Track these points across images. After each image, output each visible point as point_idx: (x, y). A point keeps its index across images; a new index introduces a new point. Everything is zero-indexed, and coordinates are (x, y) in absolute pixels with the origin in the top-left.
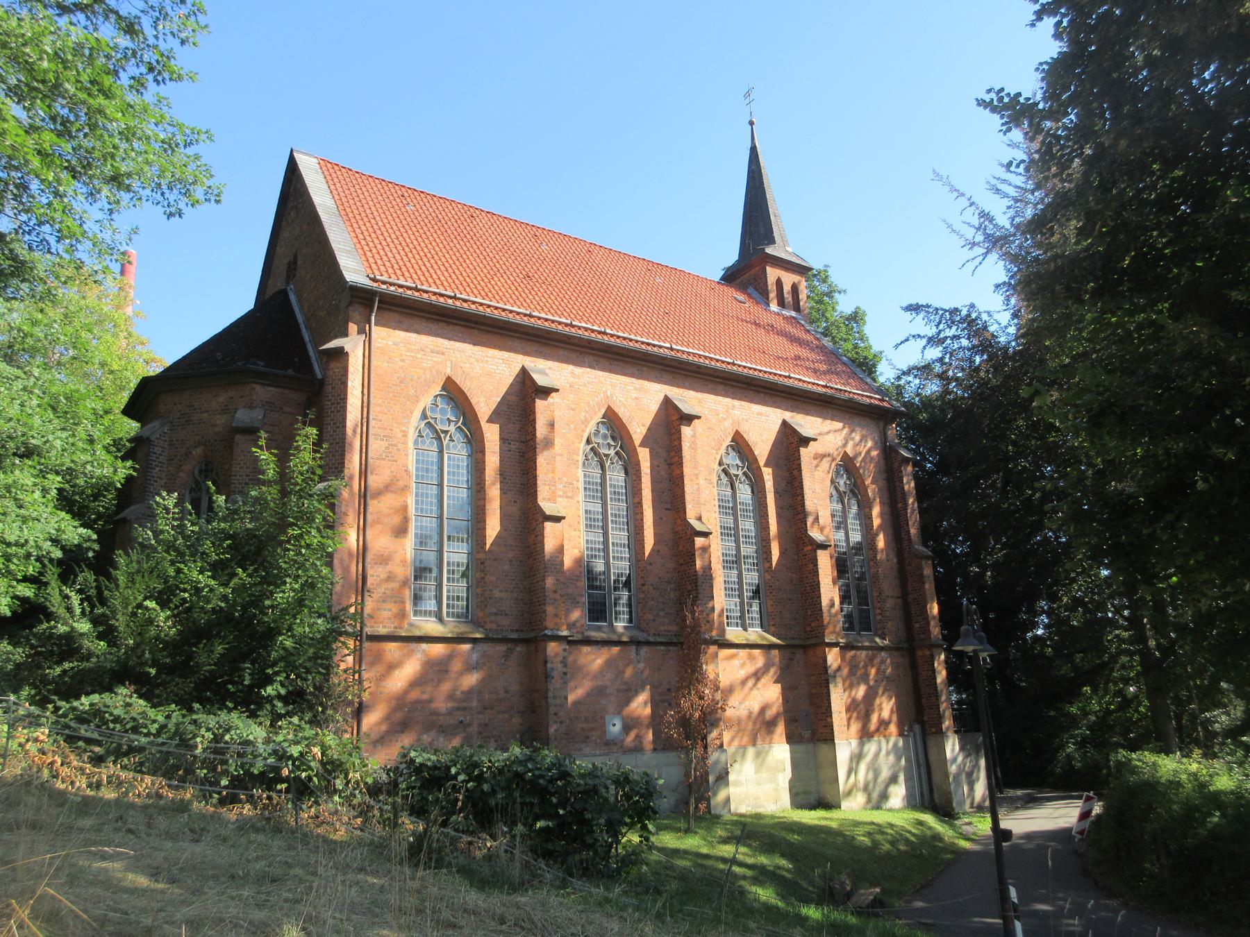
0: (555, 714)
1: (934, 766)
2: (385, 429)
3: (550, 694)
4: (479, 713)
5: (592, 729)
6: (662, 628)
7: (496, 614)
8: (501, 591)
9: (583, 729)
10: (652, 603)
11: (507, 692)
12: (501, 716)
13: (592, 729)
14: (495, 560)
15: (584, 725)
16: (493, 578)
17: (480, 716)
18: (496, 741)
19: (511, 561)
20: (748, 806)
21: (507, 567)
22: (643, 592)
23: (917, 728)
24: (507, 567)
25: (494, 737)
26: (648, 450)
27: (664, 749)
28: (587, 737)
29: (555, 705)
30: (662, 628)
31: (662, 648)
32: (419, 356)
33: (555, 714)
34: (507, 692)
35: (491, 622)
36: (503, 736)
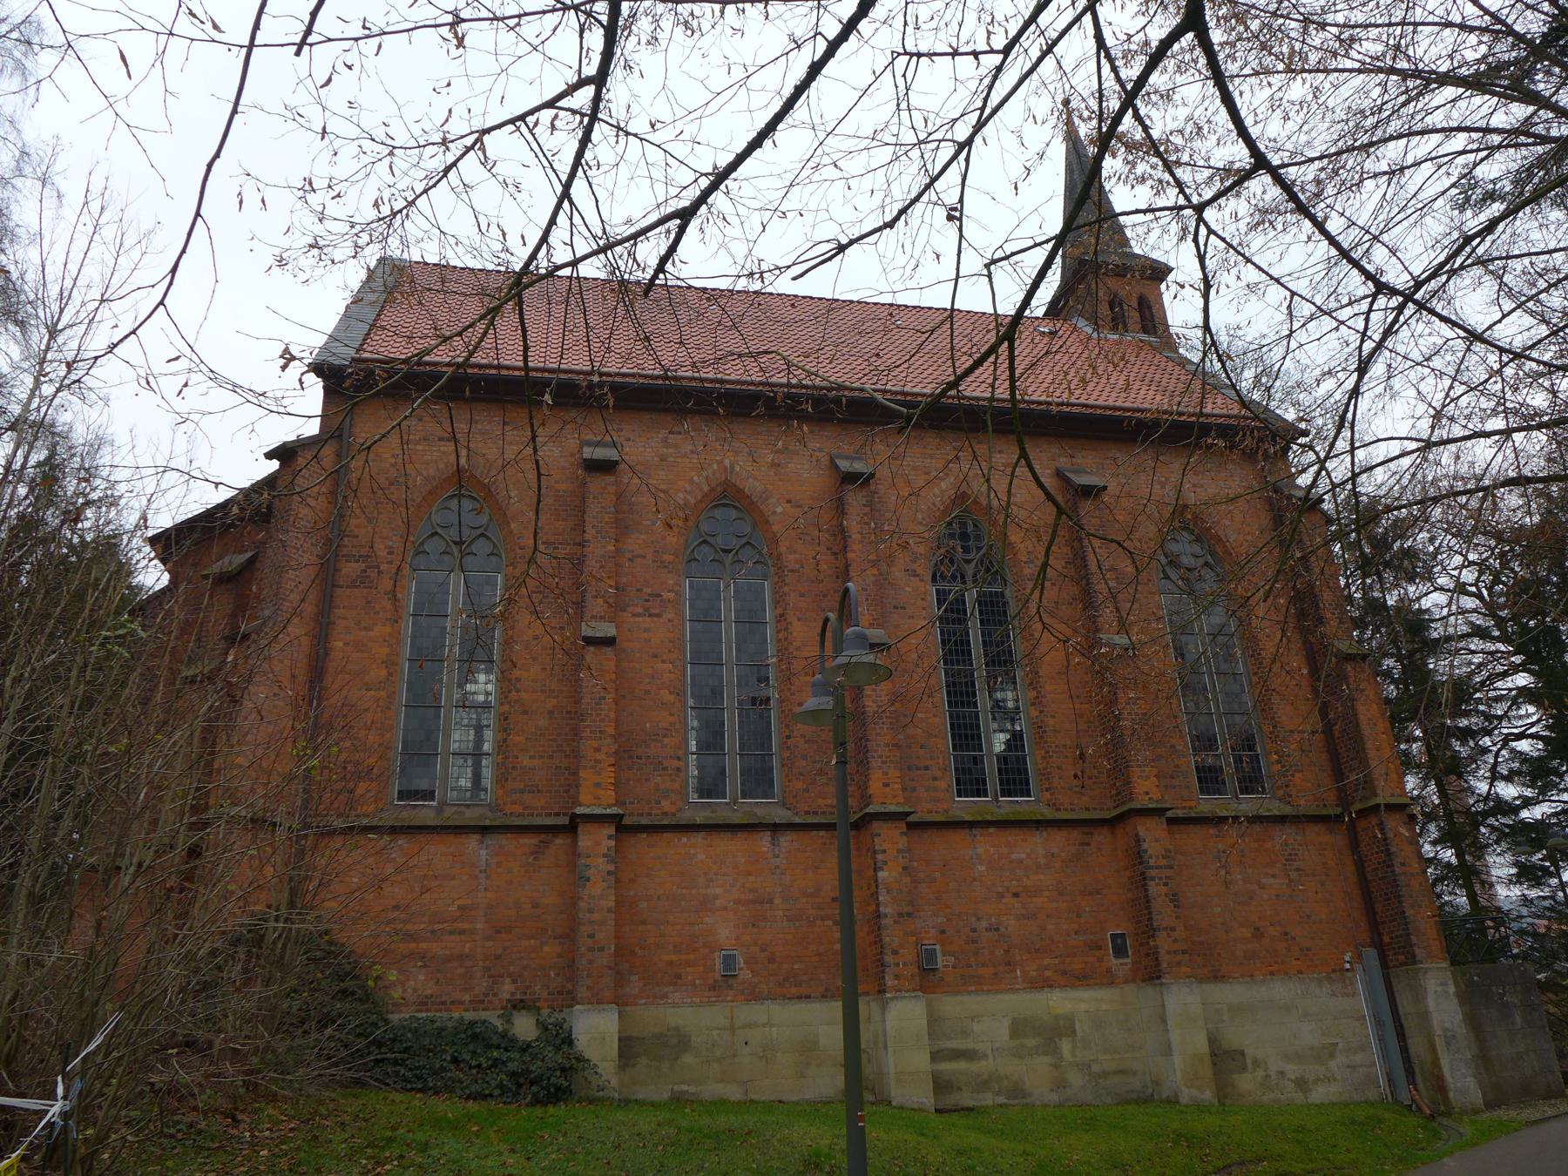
0: (591, 936)
1: (1410, 1025)
2: (363, 547)
3: (582, 905)
4: (488, 938)
5: (688, 964)
6: (821, 802)
7: (522, 791)
8: (531, 757)
9: (670, 963)
10: (803, 763)
11: (535, 905)
12: (525, 943)
13: (688, 964)
14: (525, 712)
15: (674, 957)
16: (521, 739)
17: (489, 944)
18: (514, 982)
19: (551, 713)
20: (998, 1094)
21: (543, 723)
22: (788, 748)
23: (1371, 954)
24: (543, 723)
25: (509, 975)
26: (316, 431)
27: (824, 996)
28: (679, 976)
29: (592, 923)
30: (821, 802)
31: (822, 833)
32: (420, 448)
33: (591, 936)
34: (535, 905)
35: (514, 803)
36: (526, 974)
